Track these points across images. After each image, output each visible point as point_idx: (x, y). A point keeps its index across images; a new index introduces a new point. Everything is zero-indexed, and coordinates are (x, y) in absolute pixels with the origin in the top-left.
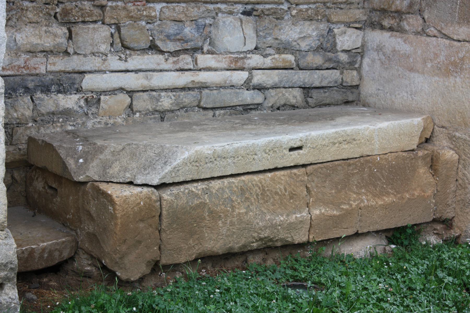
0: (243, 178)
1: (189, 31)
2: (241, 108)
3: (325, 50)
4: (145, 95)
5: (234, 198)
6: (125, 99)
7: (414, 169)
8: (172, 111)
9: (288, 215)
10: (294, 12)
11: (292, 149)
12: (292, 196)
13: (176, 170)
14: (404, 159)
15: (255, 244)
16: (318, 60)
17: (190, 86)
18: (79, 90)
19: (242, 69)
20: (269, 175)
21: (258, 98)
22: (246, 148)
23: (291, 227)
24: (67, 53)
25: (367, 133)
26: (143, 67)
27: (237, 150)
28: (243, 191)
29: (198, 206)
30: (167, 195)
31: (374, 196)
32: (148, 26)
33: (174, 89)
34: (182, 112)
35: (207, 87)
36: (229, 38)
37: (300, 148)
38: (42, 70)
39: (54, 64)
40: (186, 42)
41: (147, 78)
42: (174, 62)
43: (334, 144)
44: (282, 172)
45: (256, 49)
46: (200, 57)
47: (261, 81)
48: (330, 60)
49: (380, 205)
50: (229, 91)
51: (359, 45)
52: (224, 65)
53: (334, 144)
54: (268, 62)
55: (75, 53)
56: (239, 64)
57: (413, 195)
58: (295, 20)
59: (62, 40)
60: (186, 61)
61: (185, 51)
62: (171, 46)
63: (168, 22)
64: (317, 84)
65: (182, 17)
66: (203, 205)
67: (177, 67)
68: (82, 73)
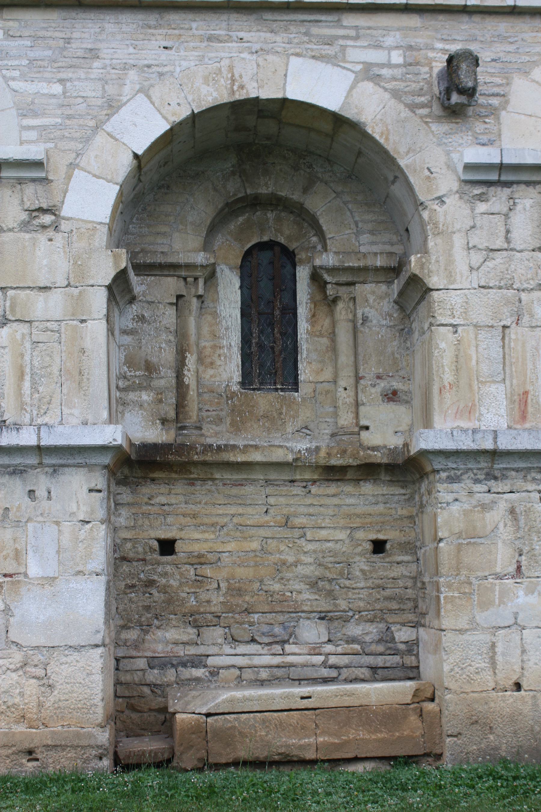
0: (265, 714)
1: (277, 630)
2: (321, 680)
3: (386, 642)
4: (249, 670)
5: (257, 725)
6: (238, 672)
7: (405, 717)
8: (270, 681)
9: (299, 740)
10: (357, 617)
11: (302, 698)
12: (303, 728)
13: (217, 705)
14: (396, 709)
15: (276, 757)
16: (381, 648)
17: (282, 665)
18: (205, 666)
19: (321, 654)
20: (286, 713)
21: (334, 673)
22: (267, 695)
23: (302, 747)
24: (197, 644)
25: (364, 690)
26: (247, 652)
27: (260, 696)
28: (264, 721)
29: (230, 728)
30: (210, 720)
31: (369, 732)
32: (250, 628)
33: (271, 667)
34: (277, 681)
35: (294, 666)
36: (307, 634)
37: (310, 697)
38: (182, 654)
39: (189, 650)
40: (276, 637)
41: (250, 659)
42: (268, 650)
43: (337, 696)
44: (295, 712)
45: (329, 641)
46: (287, 646)
47: (334, 663)
48: (390, 648)
49: (374, 739)
50: (309, 668)
51: (414, 638)
52: (305, 651)
53: (337, 696)
54: (339, 650)
55: (202, 644)
56: (317, 651)
57: (403, 734)
58: (358, 622)
59: (194, 637)
60: (277, 648)
61: (277, 643)
62: (266, 640)
63: (264, 625)
64: (381, 665)
65: (272, 621)
66: (234, 728)
67: (271, 652)
68: (208, 656)
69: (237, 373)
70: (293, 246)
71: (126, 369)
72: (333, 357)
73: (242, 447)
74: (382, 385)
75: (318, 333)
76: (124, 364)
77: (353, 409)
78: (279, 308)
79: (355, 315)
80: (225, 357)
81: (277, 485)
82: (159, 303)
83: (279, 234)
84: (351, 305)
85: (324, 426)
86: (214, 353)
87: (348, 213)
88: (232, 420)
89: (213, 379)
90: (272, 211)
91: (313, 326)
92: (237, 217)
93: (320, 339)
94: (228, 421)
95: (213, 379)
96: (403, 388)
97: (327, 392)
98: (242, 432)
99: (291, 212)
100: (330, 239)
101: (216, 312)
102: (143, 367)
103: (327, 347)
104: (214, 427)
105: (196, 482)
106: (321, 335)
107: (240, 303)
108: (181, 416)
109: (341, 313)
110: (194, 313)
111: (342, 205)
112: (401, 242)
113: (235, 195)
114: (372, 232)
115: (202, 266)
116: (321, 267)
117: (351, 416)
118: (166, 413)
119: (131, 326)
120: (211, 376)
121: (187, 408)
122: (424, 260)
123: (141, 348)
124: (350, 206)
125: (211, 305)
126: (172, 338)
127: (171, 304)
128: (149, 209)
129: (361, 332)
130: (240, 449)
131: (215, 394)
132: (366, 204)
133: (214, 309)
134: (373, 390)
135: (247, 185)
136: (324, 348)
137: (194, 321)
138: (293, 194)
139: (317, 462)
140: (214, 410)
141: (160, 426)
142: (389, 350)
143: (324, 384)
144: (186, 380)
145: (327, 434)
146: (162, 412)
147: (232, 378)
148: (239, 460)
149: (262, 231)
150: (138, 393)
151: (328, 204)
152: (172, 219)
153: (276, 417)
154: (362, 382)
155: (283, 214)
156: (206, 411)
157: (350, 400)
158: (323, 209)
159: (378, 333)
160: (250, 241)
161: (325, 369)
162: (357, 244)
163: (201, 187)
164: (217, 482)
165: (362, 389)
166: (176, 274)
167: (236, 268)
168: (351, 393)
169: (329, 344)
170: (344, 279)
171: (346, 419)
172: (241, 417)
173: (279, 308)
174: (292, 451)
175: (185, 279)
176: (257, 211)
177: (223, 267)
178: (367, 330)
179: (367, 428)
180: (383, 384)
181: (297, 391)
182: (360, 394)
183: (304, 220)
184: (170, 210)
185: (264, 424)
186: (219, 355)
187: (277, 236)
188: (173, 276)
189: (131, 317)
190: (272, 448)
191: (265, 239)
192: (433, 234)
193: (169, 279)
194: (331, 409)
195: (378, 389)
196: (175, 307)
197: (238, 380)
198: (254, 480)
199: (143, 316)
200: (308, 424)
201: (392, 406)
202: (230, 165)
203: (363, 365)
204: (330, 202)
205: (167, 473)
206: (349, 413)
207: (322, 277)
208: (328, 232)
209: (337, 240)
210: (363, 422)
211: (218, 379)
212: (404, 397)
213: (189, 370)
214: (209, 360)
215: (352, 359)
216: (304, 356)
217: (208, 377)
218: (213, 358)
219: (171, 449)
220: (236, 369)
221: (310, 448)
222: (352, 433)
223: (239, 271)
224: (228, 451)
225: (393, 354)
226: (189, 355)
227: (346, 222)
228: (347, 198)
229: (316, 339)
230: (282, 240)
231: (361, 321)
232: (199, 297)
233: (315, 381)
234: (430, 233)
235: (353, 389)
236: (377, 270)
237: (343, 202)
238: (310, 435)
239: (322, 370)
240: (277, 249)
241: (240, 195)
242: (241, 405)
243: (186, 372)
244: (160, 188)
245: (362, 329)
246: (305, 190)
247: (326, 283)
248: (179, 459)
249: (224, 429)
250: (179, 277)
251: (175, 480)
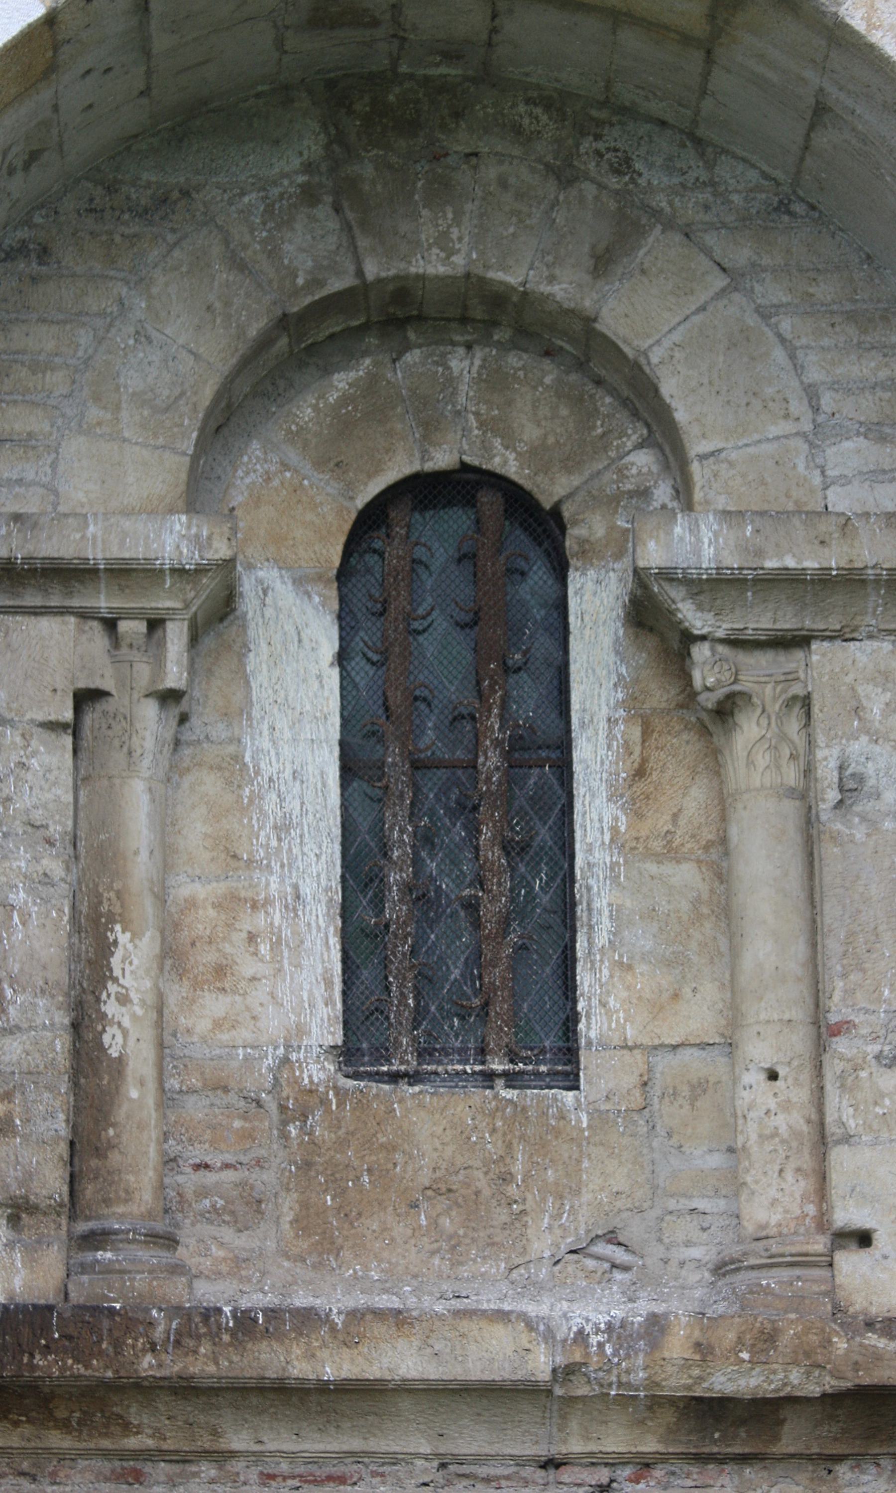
69: (323, 1011)
72: (723, 944)
73: (339, 1320)
75: (657, 845)
77: (806, 1161)
78: (497, 743)
79: (808, 772)
80: (276, 946)
81: (487, 1480)
83: (497, 442)
84: (793, 726)
85: (686, 1228)
87: (779, 354)
88: (305, 1205)
89: (225, 1037)
90: (469, 347)
92: (327, 371)
93: (668, 868)
95: (225, 1037)
97: (699, 1088)
98: (346, 1254)
100: (702, 457)
101: (237, 758)
103: (696, 903)
104: (227, 1234)
105: (148, 1468)
107: (337, 720)
108: (89, 1190)
109: (750, 763)
110: (146, 762)
111: (752, 320)
113: (315, 282)
115: (179, 572)
116: (667, 575)
118: (29, 1176)
120: (218, 1024)
121: (115, 1157)
124: (786, 325)
125: (219, 731)
126: (55, 867)
129: (835, 838)
130: (333, 1328)
132: (851, 317)
133: (231, 749)
135: (363, 242)
136: (685, 906)
137: (145, 798)
138: (551, 279)
139: (652, 1383)
140: (227, 1166)
143: (687, 1054)
145: (699, 1264)
146: (12, 1175)
147: (301, 1030)
148: (329, 1373)
151: (697, 319)
152: (57, 380)
153: (487, 1192)
154: (841, 1045)
155: (514, 360)
156: (197, 1167)
158: (676, 337)
160: (378, 470)
161: (687, 991)
162: (817, 480)
163: (177, 253)
164: (238, 1466)
165: (842, 1077)
166: (75, 602)
167: (320, 578)
169: (704, 888)
171: (774, 1202)
173: (497, 743)
174: (549, 1336)
175: (110, 625)
176: (407, 347)
177: (269, 574)
178: (859, 834)
179: (864, 1239)
183: (599, 382)
184: (50, 345)
185: (434, 1223)
186: (252, 938)
187: (487, 448)
188: (62, 611)
190: (465, 1325)
193: (46, 624)
194: (716, 1160)
196: (68, 740)
197: (330, 1041)
198: (394, 1459)
200: (617, 1222)
202: (296, 162)
203: (844, 976)
204: (703, 309)
205: (27, 1430)
206: (789, 1176)
207: (672, 613)
208: (695, 430)
209: (731, 464)
211: (244, 1034)
213: (123, 1000)
214: (207, 957)
215: (800, 949)
216: (602, 938)
217: (203, 1026)
218: (228, 949)
219: (46, 1329)
220: (320, 992)
221: (623, 1324)
222: (802, 1261)
223: (333, 593)
224: (280, 1337)
226: (124, 938)
227: (769, 391)
229: (652, 867)
231: (833, 796)
233: (647, 1041)
235: (806, 1076)
237: (758, 310)
238: (626, 1268)
239: (676, 996)
241: (336, 285)
242: (342, 1144)
243: (111, 1008)
245: (839, 826)
247: (689, 638)
248: (79, 1369)
249: (271, 1245)
250: (84, 615)
251: (62, 1457)
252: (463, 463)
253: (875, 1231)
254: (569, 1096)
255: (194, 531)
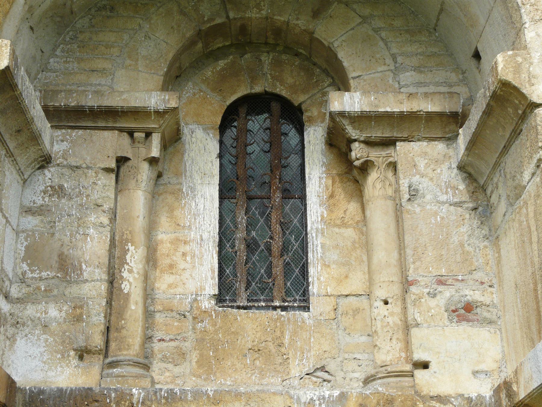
69: (211, 281)
70: (297, 99)
71: (25, 267)
72: (365, 258)
73: (211, 394)
74: (447, 294)
75: (338, 222)
76: (23, 260)
77: (400, 335)
79: (397, 191)
80: (193, 256)
82: (88, 168)
83: (278, 84)
84: (390, 174)
85: (353, 365)
86: (175, 250)
87: (381, 44)
88: (201, 355)
90: (268, 52)
91: (330, 210)
93: (343, 230)
94: (194, 356)
96: (481, 299)
97: (357, 311)
98: (218, 375)
99: (297, 54)
100: (354, 78)
102: (55, 265)
103: (354, 242)
104: (170, 366)
106: (344, 225)
108: (113, 345)
109: (374, 186)
110: (143, 184)
111: (371, 32)
112: (464, 81)
113: (211, 20)
114: (418, 69)
115: (157, 112)
116: (342, 114)
117: (398, 345)
119: (40, 202)
120: (170, 286)
121: (124, 332)
122: (519, 59)
123: (53, 235)
124: (383, 34)
127: (108, 170)
128: (81, 37)
129: (408, 211)
130: (208, 396)
131: (174, 314)
132: (407, 31)
133: (178, 187)
134: (432, 303)
135: (229, 6)
136: (349, 244)
138: (298, 19)
140: (171, 340)
141: (75, 362)
142: (455, 239)
143: (351, 299)
144: (126, 287)
145: (358, 380)
147: (202, 288)
149: (253, 79)
150: (41, 307)
151: (351, 32)
152: (115, 51)
153: (274, 351)
154: (413, 289)
155: (284, 57)
156: (160, 340)
157: (395, 320)
158: (343, 38)
159: (436, 214)
160: (235, 92)
161: (351, 275)
162: (397, 86)
163: (161, 10)
165: (414, 301)
166: (118, 125)
168: (395, 307)
169: (356, 237)
170: (377, 134)
171: (388, 352)
172: (216, 350)
175: (131, 134)
176: (246, 53)
178: (418, 210)
179: (425, 366)
180: (447, 293)
181: (306, 308)
182: (411, 310)
183: (315, 64)
184: (113, 39)
186: (184, 254)
187: (274, 86)
189: (42, 188)
191: (258, 89)
192: (533, 20)
193: (106, 133)
194: (364, 339)
195: (441, 301)
196: (113, 176)
197: (213, 293)
199: (61, 187)
201: (464, 328)
203: (414, 263)
204: (353, 29)
206: (394, 341)
207: (344, 130)
208: (351, 69)
209: (365, 81)
210: (419, 355)
211: (180, 290)
212: (486, 314)
213: (130, 271)
215: (395, 255)
218: (175, 258)
220: (209, 274)
222: (401, 374)
223: (218, 132)
225: (462, 245)
226: (132, 248)
227: (378, 56)
228: (378, 23)
229: (336, 230)
230: (284, 93)
231: (407, 196)
232: (153, 161)
233: (336, 293)
234: (525, 18)
235: (399, 303)
236: (430, 116)
237: (374, 30)
238: (329, 381)
239: (347, 277)
240: (275, 106)
241: (219, 21)
242: (216, 332)
243: (125, 274)
244: (99, 9)
245: (410, 207)
246: (316, 14)
247: (350, 141)
249: (188, 371)
252: (265, 91)
253: (430, 362)
254: (306, 314)
255: (163, 97)
